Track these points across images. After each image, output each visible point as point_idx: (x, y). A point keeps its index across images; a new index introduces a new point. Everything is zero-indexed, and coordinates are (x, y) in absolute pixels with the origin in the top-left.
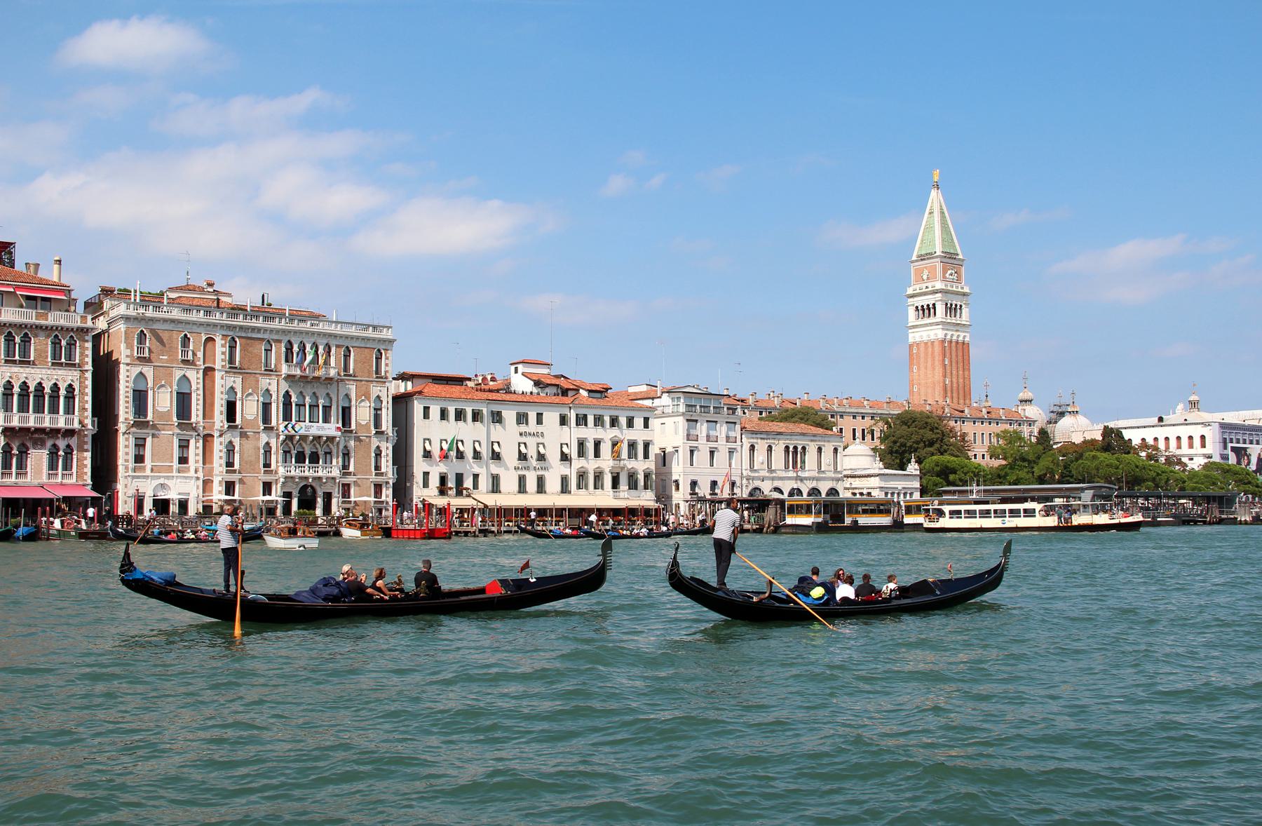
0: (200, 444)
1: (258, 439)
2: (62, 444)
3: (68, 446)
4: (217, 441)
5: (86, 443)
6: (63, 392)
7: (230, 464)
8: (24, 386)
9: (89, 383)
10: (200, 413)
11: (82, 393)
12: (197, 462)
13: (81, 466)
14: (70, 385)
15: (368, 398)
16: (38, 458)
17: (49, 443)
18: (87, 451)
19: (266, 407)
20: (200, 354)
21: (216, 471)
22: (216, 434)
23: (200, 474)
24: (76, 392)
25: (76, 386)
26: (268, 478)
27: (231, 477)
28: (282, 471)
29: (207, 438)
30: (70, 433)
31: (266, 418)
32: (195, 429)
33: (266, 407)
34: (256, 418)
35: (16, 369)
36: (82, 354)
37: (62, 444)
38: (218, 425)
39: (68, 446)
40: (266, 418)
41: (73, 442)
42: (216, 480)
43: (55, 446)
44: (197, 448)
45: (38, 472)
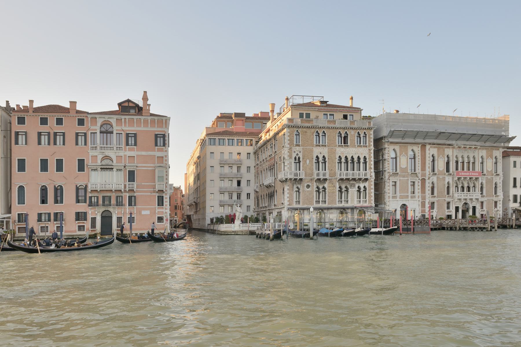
0: (420, 184)
1: (445, 180)
2: (362, 185)
3: (364, 187)
4: (427, 181)
5: (372, 185)
6: (362, 160)
7: (433, 193)
8: (346, 158)
9: (372, 155)
10: (420, 168)
11: (370, 161)
12: (419, 193)
13: (370, 196)
14: (365, 157)
16: (353, 191)
17: (357, 186)
18: (372, 189)
19: (448, 163)
21: (427, 197)
22: (427, 178)
23: (420, 199)
24: (367, 160)
25: (367, 157)
27: (433, 200)
28: (456, 195)
29: (423, 181)
30: (366, 180)
31: (448, 170)
33: (448, 163)
35: (342, 149)
36: (369, 141)
37: (362, 185)
38: (427, 173)
39: (364, 187)
40: (448, 170)
41: (366, 184)
43: (359, 187)
44: (419, 186)
45: (353, 200)
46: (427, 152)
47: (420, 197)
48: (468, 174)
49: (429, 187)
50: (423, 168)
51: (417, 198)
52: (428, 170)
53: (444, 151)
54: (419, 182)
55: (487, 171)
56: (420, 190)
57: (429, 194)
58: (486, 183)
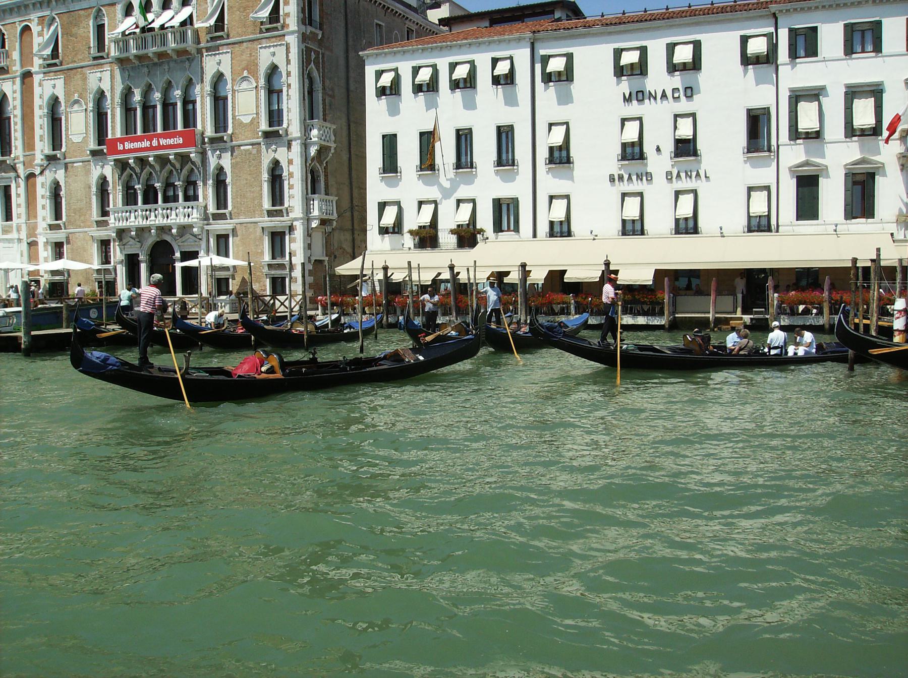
0: (22, 190)
1: (88, 172)
4: (40, 180)
15: (254, 72)
20: (16, 55)
23: (23, 235)
26: (103, 234)
32: (14, 169)
34: (85, 140)
42: (41, 240)
46: (37, 90)
47: (24, 227)
48: (146, 144)
49: (43, 197)
50: (29, 145)
51: (14, 235)
52: (42, 147)
53: (85, 79)
54: (18, 186)
55: (238, 124)
56: (23, 210)
57: (44, 220)
58: (233, 166)
